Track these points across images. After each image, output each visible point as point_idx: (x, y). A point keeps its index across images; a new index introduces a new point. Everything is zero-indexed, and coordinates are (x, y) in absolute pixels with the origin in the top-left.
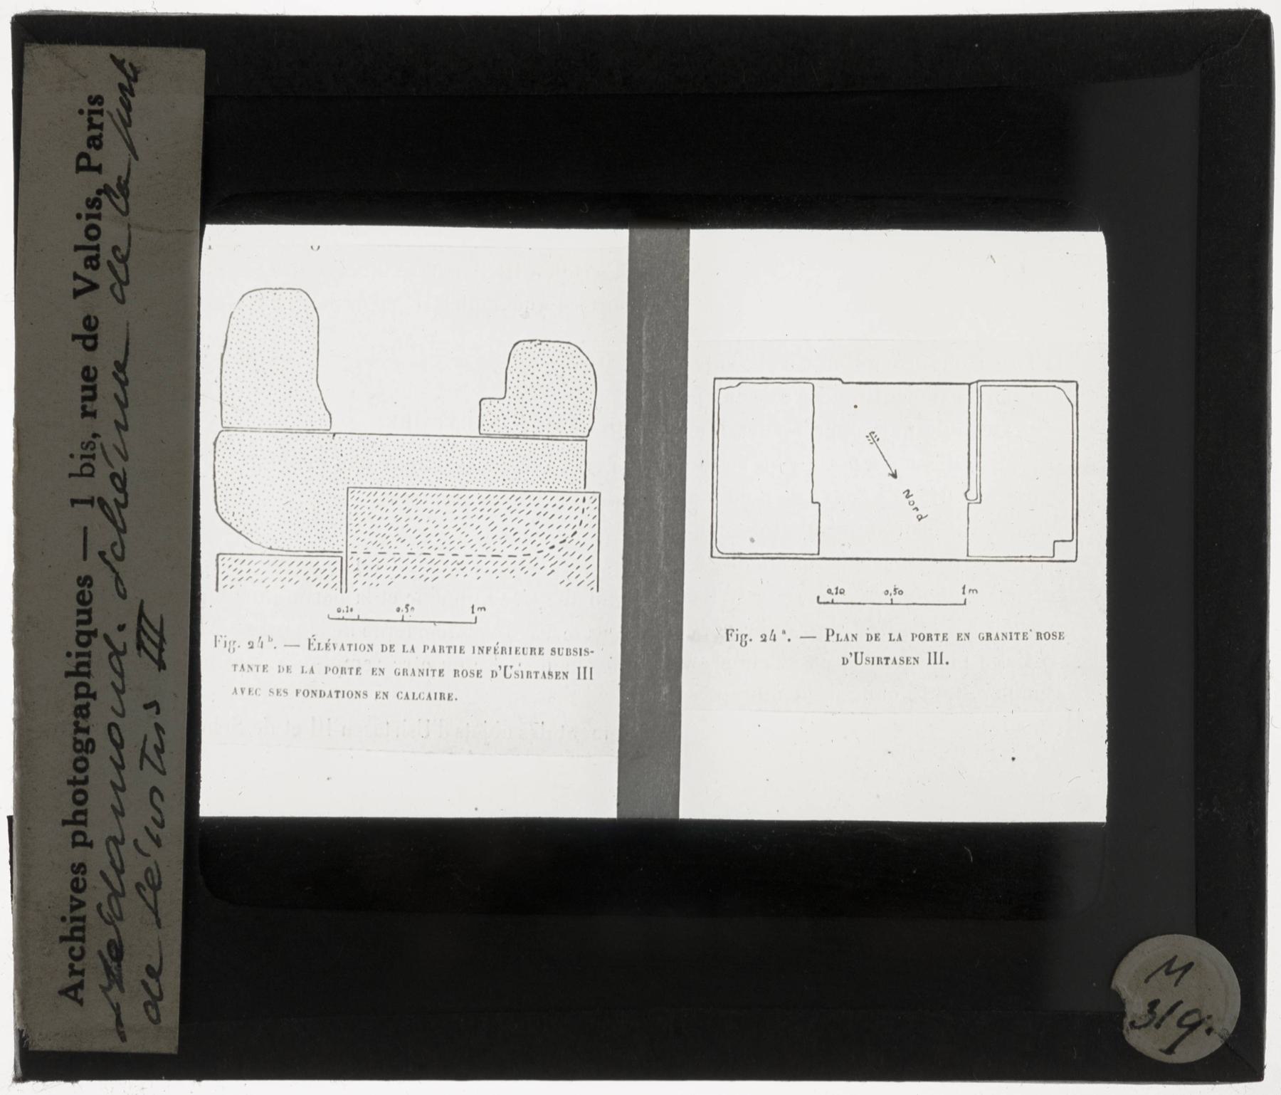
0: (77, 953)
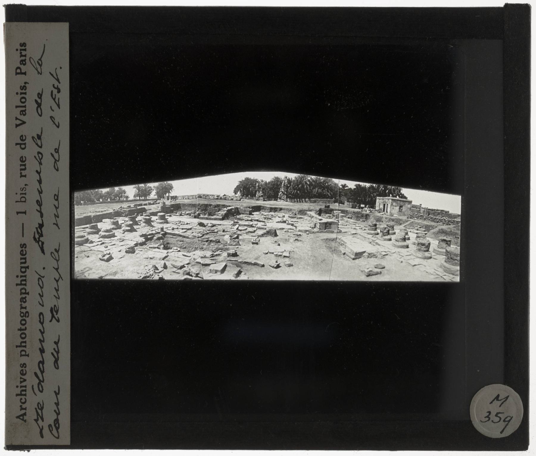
0: (23, 401)
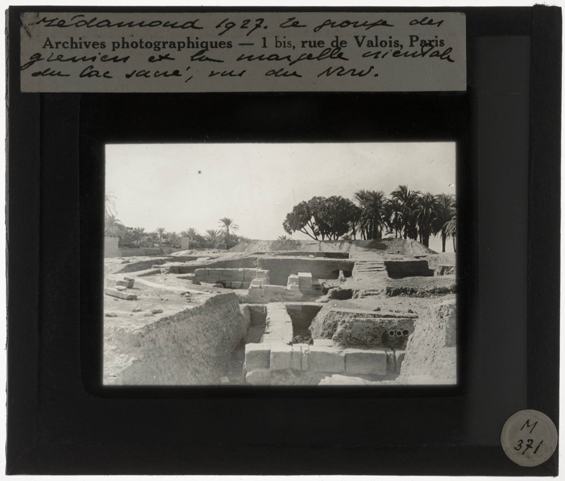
0: (66, 45)
